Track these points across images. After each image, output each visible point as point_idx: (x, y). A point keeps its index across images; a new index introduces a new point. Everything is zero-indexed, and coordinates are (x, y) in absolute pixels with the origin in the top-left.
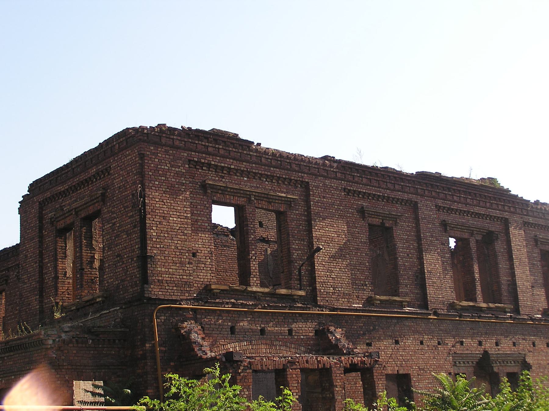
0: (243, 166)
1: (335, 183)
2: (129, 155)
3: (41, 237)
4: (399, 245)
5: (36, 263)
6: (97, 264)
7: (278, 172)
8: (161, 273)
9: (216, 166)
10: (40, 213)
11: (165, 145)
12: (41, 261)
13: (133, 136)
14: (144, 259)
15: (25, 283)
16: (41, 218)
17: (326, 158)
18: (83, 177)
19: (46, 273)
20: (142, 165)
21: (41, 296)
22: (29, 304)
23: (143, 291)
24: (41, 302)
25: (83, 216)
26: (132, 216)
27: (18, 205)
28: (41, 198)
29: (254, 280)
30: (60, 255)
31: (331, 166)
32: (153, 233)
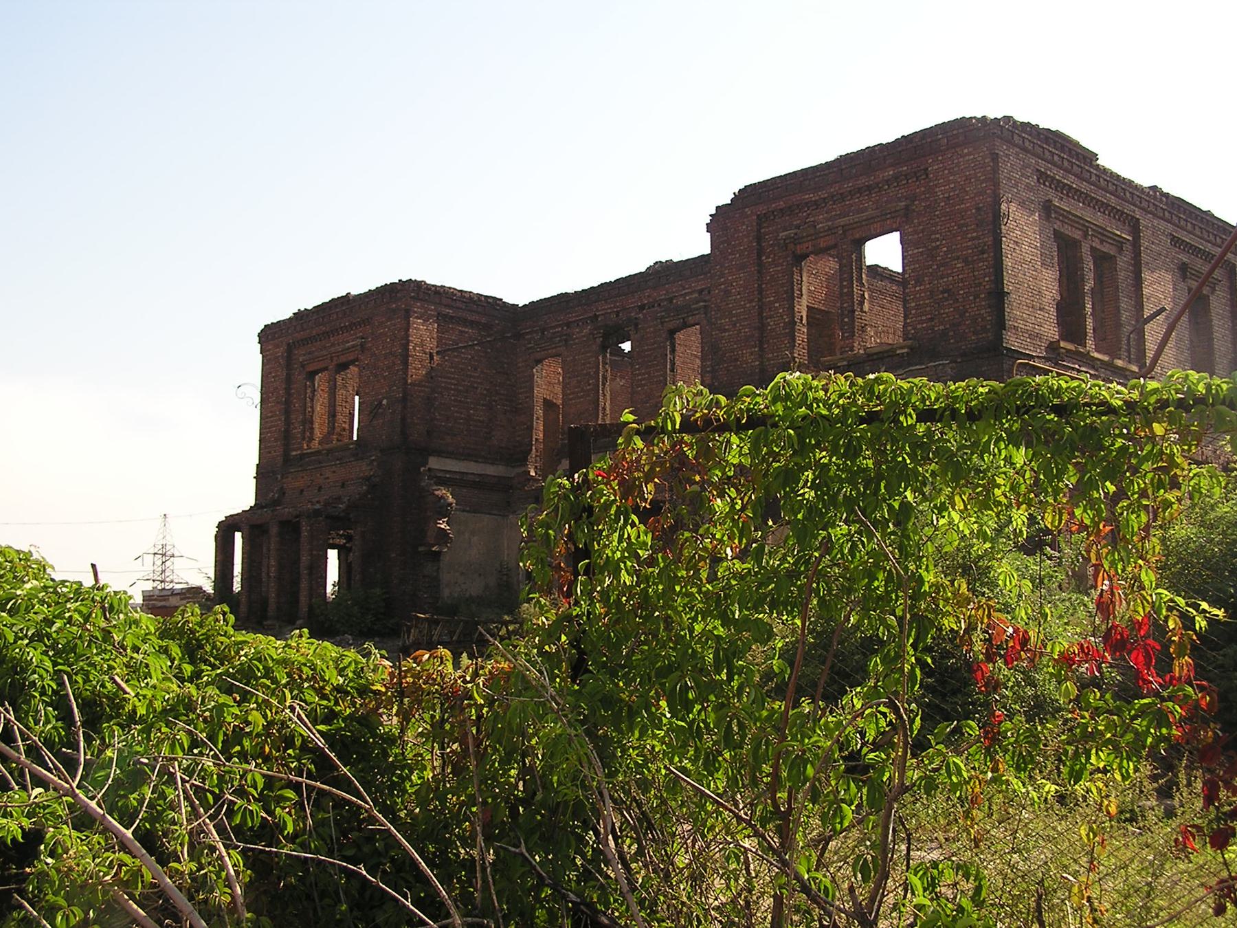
0: (1084, 187)
1: (1163, 225)
2: (969, 154)
3: (760, 264)
4: (1215, 322)
5: (751, 301)
6: (866, 306)
7: (1113, 201)
8: (1016, 320)
9: (1059, 181)
10: (759, 231)
11: (1016, 146)
12: (760, 300)
13: (979, 129)
14: (998, 296)
15: (728, 330)
16: (759, 238)
17: (1154, 188)
18: (862, 181)
19: (770, 317)
20: (995, 170)
21: (762, 349)
22: (736, 360)
23: (1000, 339)
24: (761, 356)
25: (857, 236)
26: (977, 238)
27: (708, 220)
28: (762, 209)
29: (1090, 343)
30: (797, 292)
31: (1161, 202)
32: (1008, 262)
